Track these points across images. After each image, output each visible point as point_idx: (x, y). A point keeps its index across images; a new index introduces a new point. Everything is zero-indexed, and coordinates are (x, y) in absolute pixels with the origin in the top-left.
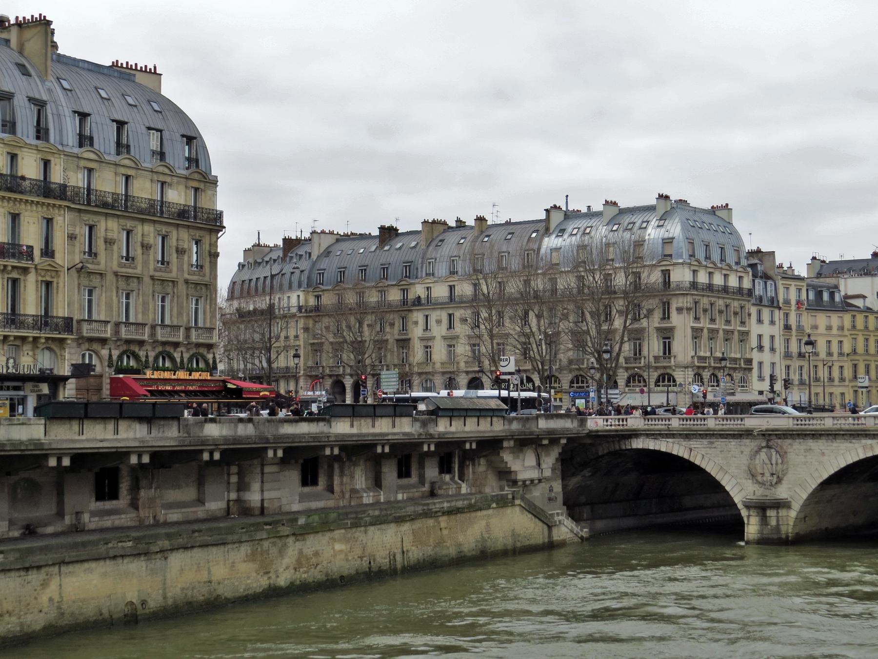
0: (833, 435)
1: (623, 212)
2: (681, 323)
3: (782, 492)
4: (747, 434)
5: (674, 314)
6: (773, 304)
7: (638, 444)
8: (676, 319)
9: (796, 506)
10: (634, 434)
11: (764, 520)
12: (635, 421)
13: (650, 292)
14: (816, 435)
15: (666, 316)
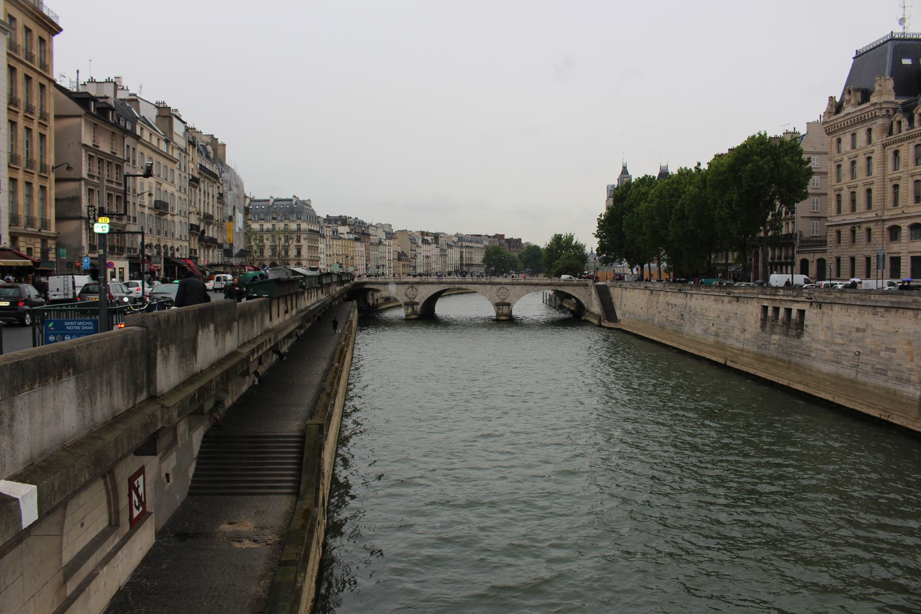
0: (432, 283)
1: (276, 200)
2: (304, 243)
3: (416, 300)
4: (406, 283)
5: (302, 240)
6: (323, 236)
7: (367, 286)
8: (303, 242)
9: (421, 304)
10: (366, 283)
11: (413, 309)
12: (365, 279)
13: (293, 232)
14: (428, 283)
15: (299, 241)
